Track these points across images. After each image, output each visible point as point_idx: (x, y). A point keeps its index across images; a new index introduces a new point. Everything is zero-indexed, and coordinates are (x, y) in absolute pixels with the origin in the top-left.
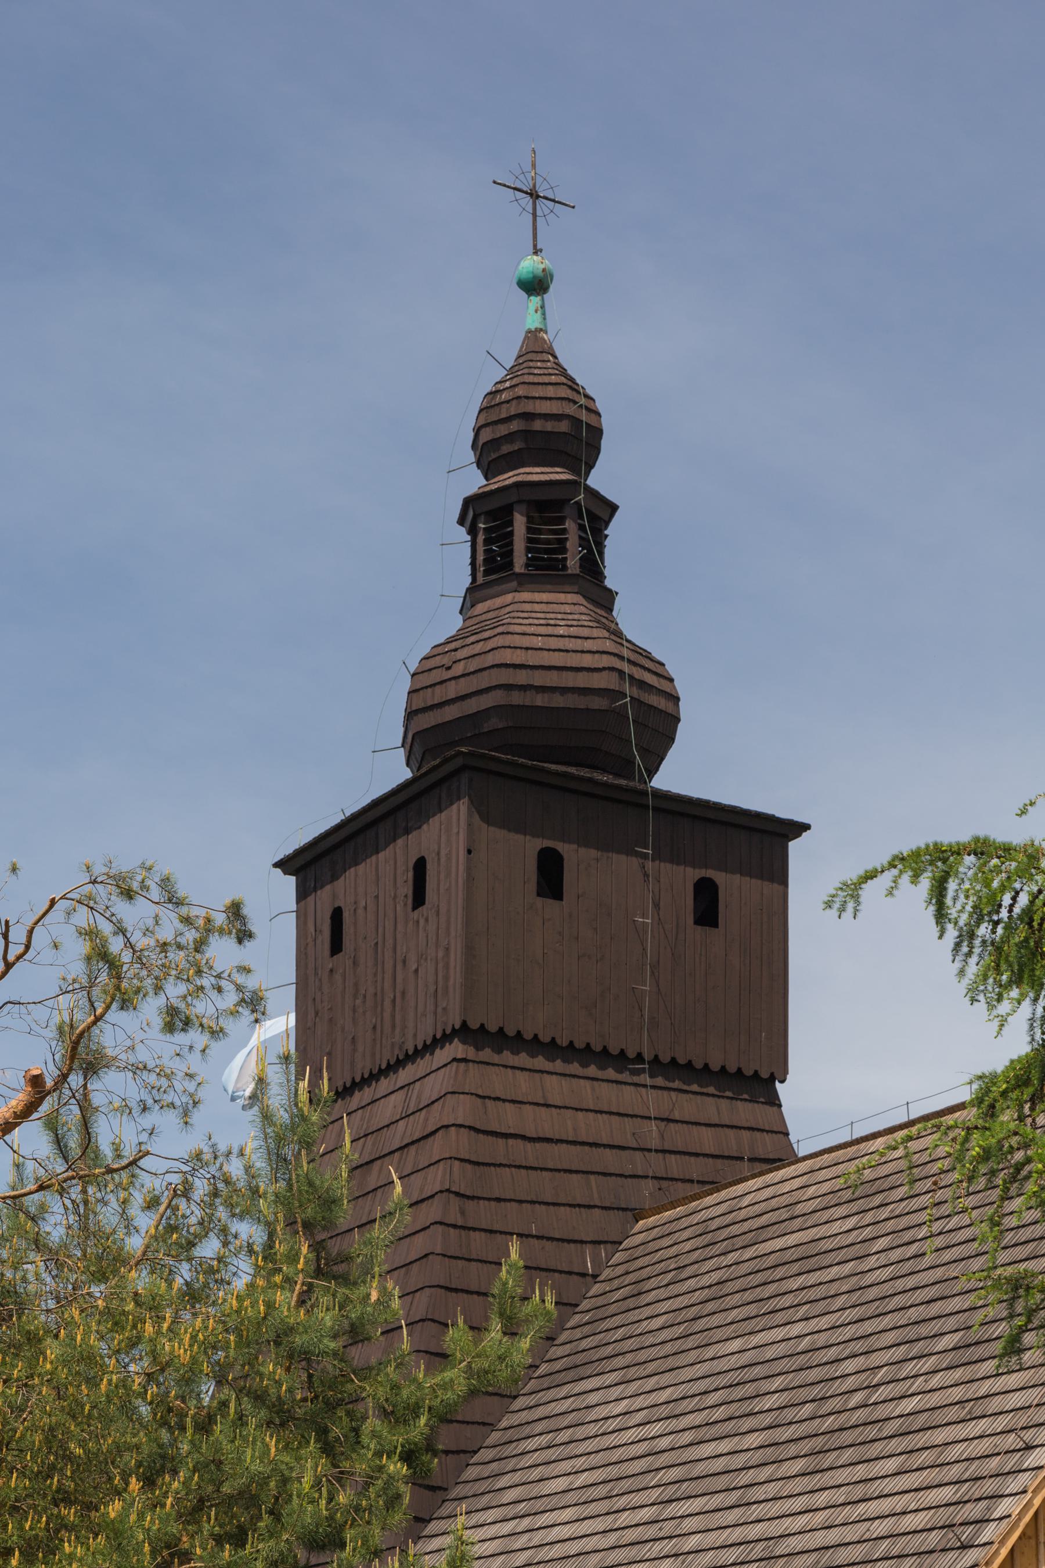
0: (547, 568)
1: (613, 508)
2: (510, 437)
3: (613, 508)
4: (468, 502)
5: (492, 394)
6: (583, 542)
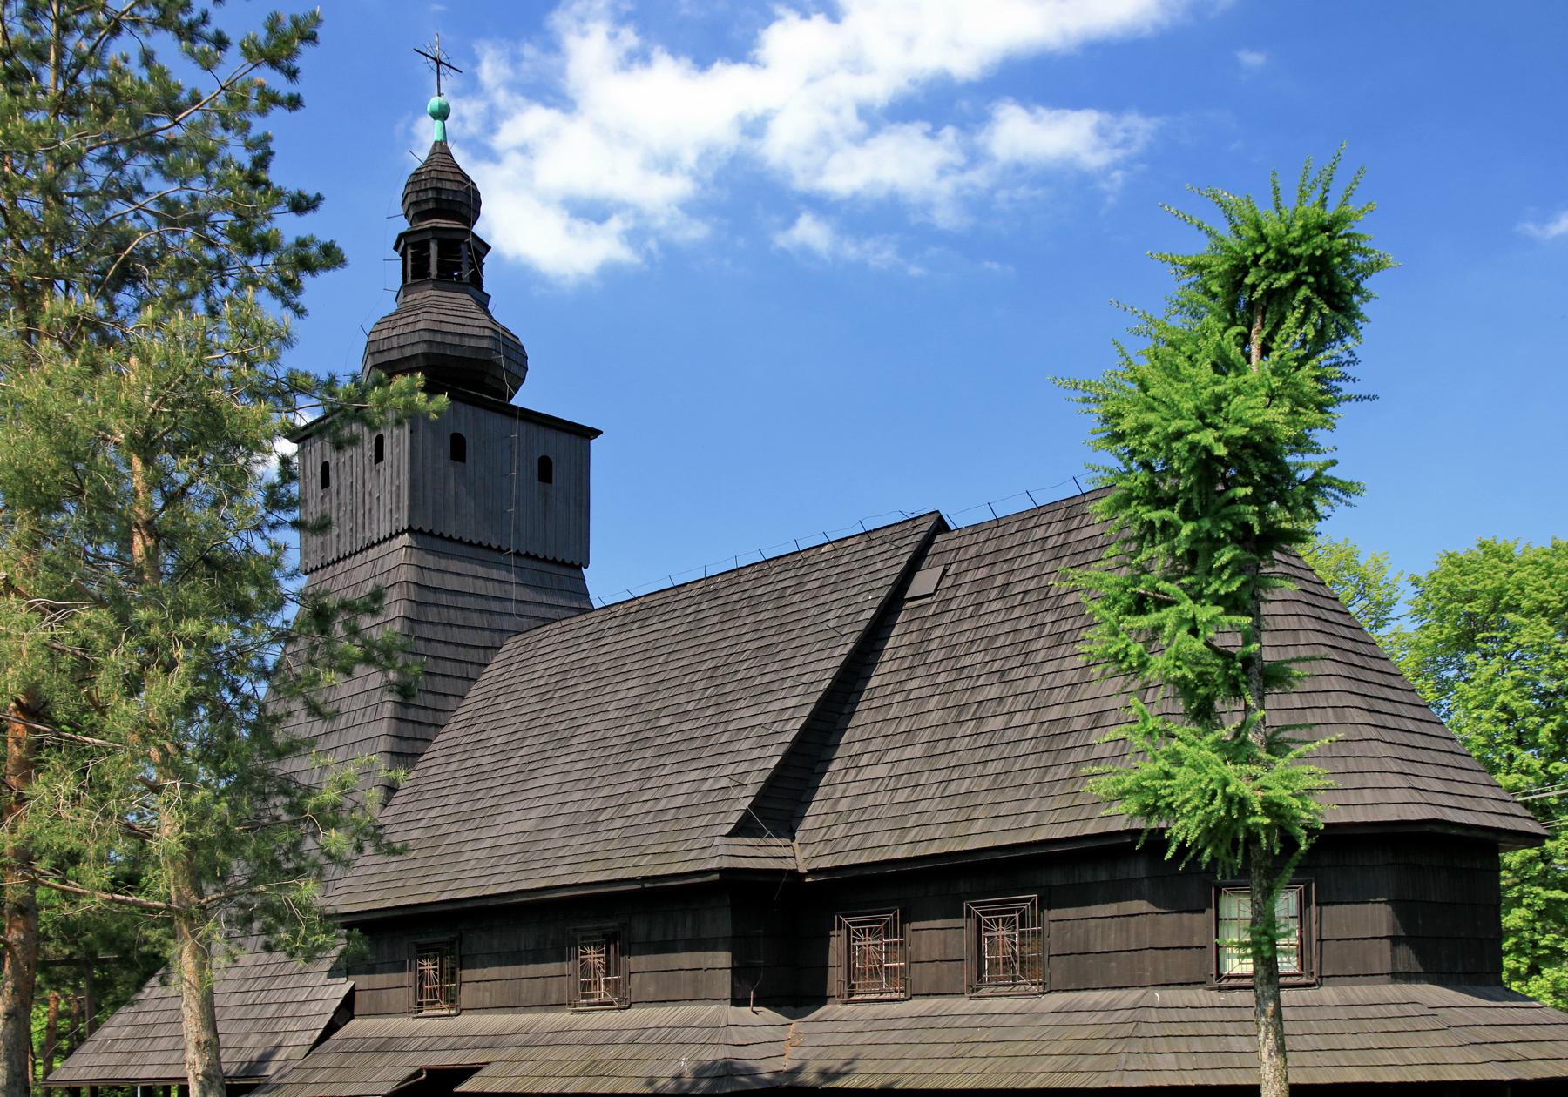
0: (447, 278)
2: (427, 200)
3: (488, 248)
4: (401, 236)
5: (415, 174)
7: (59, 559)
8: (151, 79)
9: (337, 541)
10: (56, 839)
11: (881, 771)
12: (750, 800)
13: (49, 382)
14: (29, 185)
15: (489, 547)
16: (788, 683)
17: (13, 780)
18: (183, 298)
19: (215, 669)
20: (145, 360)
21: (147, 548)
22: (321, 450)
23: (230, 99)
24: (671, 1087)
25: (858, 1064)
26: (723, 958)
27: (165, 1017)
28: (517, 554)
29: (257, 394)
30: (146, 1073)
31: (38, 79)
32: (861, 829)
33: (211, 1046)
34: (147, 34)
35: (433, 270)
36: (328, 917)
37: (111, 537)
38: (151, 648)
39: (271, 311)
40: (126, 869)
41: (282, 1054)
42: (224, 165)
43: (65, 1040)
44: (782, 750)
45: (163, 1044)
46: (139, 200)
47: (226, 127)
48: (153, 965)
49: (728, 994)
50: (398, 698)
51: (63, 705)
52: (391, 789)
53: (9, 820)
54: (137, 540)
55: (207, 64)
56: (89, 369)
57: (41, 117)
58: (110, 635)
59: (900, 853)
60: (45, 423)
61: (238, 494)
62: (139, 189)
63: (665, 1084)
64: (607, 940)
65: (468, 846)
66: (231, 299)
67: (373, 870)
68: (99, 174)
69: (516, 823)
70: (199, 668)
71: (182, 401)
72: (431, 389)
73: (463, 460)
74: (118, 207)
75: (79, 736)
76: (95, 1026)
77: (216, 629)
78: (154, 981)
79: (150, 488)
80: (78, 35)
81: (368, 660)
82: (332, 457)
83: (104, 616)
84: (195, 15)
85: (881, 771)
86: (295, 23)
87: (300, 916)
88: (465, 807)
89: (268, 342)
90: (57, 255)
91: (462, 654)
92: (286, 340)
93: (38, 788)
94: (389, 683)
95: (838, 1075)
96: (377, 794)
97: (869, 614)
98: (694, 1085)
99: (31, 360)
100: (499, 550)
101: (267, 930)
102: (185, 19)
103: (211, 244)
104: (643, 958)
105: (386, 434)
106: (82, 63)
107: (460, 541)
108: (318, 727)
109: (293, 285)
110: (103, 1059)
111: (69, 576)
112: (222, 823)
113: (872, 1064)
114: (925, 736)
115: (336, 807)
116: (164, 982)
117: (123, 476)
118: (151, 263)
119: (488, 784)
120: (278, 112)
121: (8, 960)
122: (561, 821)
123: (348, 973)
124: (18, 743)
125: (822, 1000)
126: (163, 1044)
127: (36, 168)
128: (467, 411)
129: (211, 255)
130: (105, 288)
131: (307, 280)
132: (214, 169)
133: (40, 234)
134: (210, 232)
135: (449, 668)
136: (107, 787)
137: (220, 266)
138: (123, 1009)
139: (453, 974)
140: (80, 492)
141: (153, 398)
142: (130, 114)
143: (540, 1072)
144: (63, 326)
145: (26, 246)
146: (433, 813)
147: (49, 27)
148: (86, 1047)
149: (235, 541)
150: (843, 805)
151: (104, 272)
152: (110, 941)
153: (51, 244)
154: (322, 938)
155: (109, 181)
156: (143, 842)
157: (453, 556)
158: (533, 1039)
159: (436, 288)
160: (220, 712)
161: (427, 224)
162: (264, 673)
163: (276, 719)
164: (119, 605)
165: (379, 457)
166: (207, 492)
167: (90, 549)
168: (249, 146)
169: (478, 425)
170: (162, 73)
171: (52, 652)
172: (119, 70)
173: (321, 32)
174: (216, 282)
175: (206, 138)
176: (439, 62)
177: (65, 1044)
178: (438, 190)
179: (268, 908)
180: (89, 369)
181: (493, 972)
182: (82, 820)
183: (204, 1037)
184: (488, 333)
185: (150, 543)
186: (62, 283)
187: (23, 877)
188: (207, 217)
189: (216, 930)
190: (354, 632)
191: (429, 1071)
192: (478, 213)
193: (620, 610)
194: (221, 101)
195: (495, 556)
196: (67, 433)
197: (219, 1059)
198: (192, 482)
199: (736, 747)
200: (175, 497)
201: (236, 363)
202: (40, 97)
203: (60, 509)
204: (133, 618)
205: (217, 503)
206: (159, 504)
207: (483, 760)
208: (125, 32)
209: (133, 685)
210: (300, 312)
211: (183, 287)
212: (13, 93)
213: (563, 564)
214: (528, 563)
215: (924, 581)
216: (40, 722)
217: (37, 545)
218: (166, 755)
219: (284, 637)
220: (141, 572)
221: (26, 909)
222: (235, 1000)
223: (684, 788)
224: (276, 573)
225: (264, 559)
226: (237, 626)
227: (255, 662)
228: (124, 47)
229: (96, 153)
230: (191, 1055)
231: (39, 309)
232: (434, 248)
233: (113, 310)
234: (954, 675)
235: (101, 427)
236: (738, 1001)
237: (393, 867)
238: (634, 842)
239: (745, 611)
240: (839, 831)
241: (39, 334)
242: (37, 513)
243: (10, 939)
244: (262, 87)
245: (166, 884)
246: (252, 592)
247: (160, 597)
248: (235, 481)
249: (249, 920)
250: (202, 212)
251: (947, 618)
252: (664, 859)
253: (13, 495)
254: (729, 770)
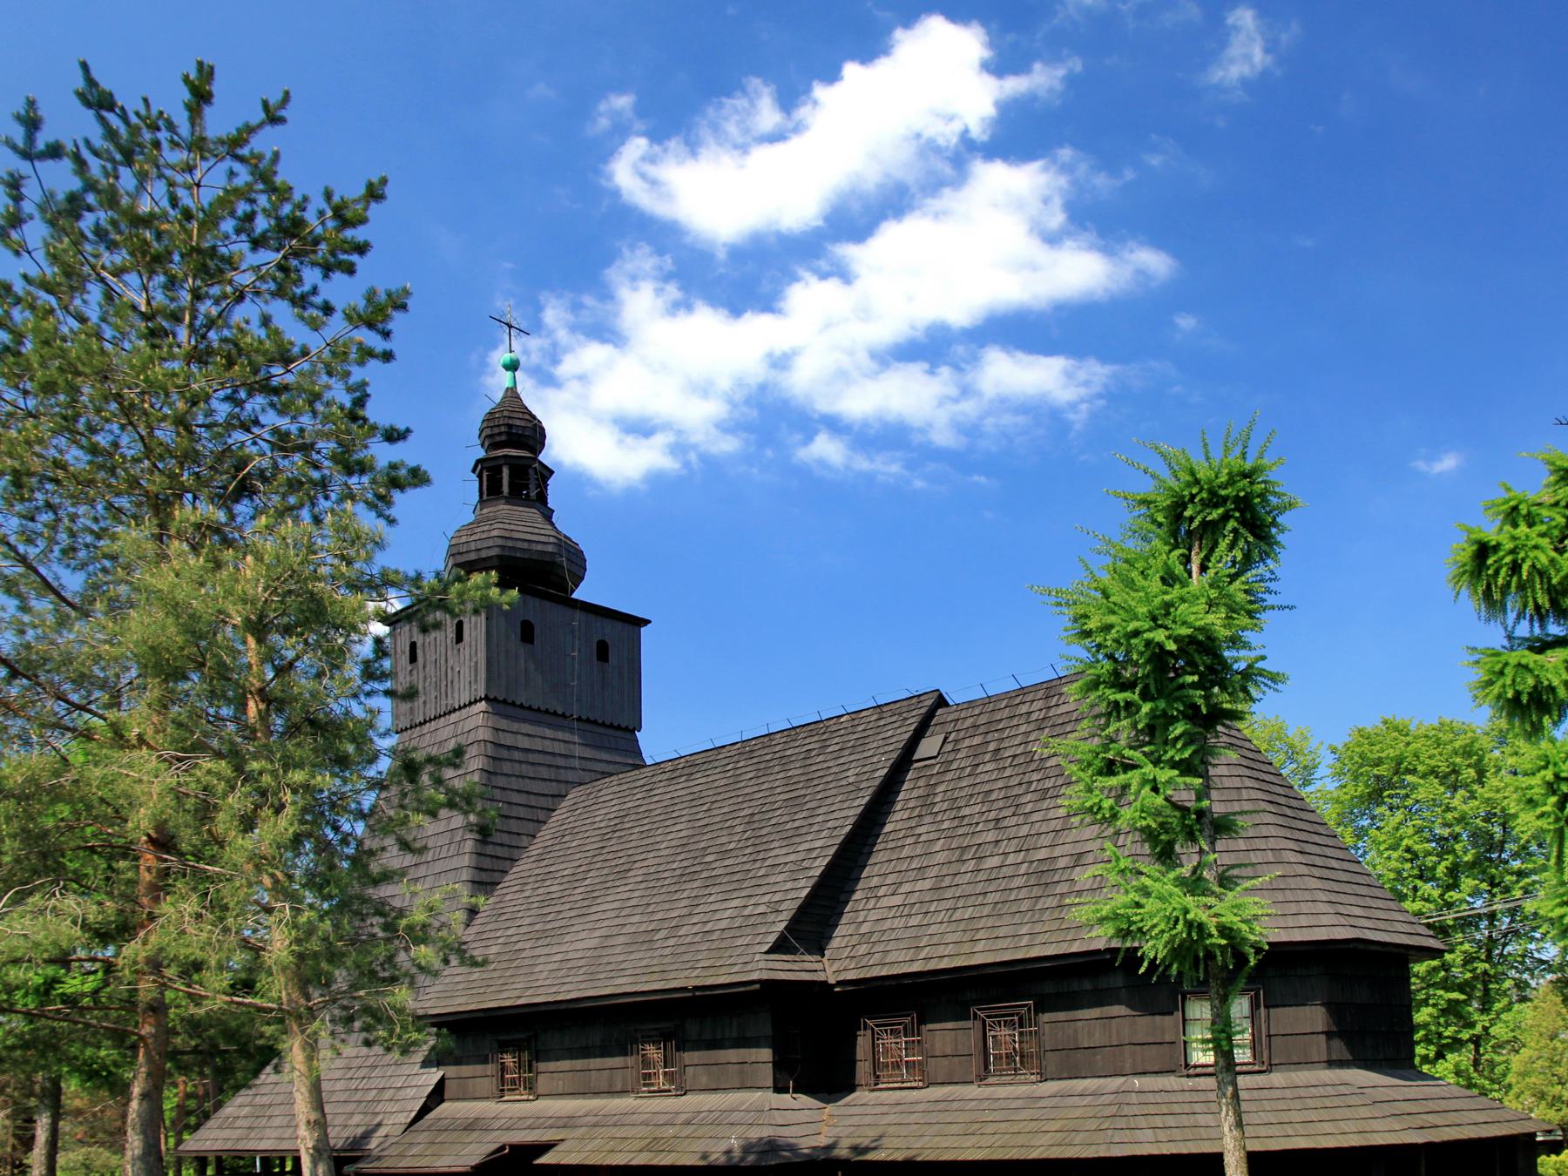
0: (517, 495)
1: (552, 472)
2: (500, 434)
3: (552, 472)
4: (478, 462)
6: (539, 486)
7: (184, 718)
8: (268, 336)
9: (421, 708)
10: (183, 951)
11: (897, 900)
12: (784, 924)
13: (177, 575)
14: (164, 418)
15: (555, 714)
16: (816, 828)
17: (145, 901)
18: (291, 508)
19: (319, 811)
20: (259, 558)
21: (259, 711)
22: (408, 632)
23: (333, 353)
24: (722, 1160)
25: (885, 1141)
26: (766, 1054)
27: (279, 1099)
28: (579, 719)
29: (355, 586)
30: (263, 1145)
31: (175, 336)
32: (881, 947)
33: (320, 1124)
34: (266, 302)
35: (506, 489)
36: (420, 1018)
37: (229, 701)
38: (263, 793)
39: (367, 521)
40: (243, 975)
41: (382, 1132)
42: (328, 404)
43: (195, 1116)
44: (812, 882)
45: (277, 1121)
46: (256, 430)
47: (330, 374)
48: (268, 1055)
49: (770, 1083)
50: (477, 837)
51: (188, 839)
52: (473, 912)
53: (142, 934)
54: (251, 704)
55: (315, 326)
56: (211, 565)
57: (176, 366)
58: (228, 781)
59: (916, 967)
60: (174, 608)
61: (338, 667)
62: (256, 422)
63: (717, 1158)
64: (663, 1038)
65: (541, 960)
66: (333, 511)
67: (458, 979)
68: (222, 410)
69: (581, 941)
70: (305, 810)
71: (290, 592)
72: (504, 584)
73: (532, 642)
74: (239, 436)
75: (202, 865)
76: (218, 1106)
77: (319, 778)
78: (269, 1069)
79: (263, 662)
80: (209, 303)
81: (451, 805)
82: (419, 638)
83: (223, 766)
84: (307, 288)
85: (897, 900)
86: (389, 295)
87: (395, 1017)
88: (537, 927)
89: (364, 545)
90: (186, 474)
91: (533, 801)
92: (379, 544)
93: (166, 908)
94: (470, 824)
95: (867, 1150)
96: (461, 916)
97: (883, 772)
98: (742, 1159)
99: (163, 557)
100: (564, 716)
101: (367, 1028)
102: (298, 291)
103: (316, 467)
104: (696, 1054)
105: (466, 620)
106: (211, 323)
107: (530, 708)
108: (409, 859)
109: (385, 500)
110: (227, 1133)
111: (193, 733)
112: (325, 939)
113: (896, 1140)
114: (934, 872)
115: (424, 926)
116: (277, 1070)
117: (239, 652)
118: (265, 480)
119: (557, 908)
120: (373, 364)
121: (142, 1052)
122: (621, 939)
123: (439, 1064)
124: (149, 869)
125: (851, 1087)
126: (277, 1121)
127: (171, 405)
128: (535, 602)
129: (316, 475)
130: (227, 499)
131: (397, 496)
132: (320, 408)
133: (172, 457)
134: (315, 457)
136: (225, 908)
137: (323, 484)
138: (243, 1092)
139: (530, 1066)
140: (203, 665)
141: (265, 590)
142: (250, 364)
143: (608, 1147)
144: (190, 530)
145: (160, 466)
146: (510, 932)
147: (186, 297)
148: (210, 1123)
149: (335, 706)
150: (864, 928)
151: (225, 488)
152: (230, 1035)
153: (181, 465)
154: (415, 1036)
155: (231, 416)
156: (258, 957)
157: (524, 720)
158: (600, 1122)
159: (508, 503)
160: (323, 847)
161: (500, 453)
162: (361, 815)
163: (371, 853)
164: (236, 757)
165: (459, 638)
166: (312, 666)
167: (211, 711)
168: (349, 390)
169: (544, 614)
170: (277, 332)
171: (179, 796)
172: (241, 330)
173: (410, 302)
174: (320, 496)
175: (314, 383)
176: (510, 327)
177: (192, 1120)
178: (510, 426)
179: (367, 1010)
180: (211, 565)
181: (565, 1064)
182: (204, 935)
183: (313, 1116)
184: (552, 540)
185: (262, 706)
186: (190, 496)
187: (154, 981)
188: (313, 445)
189: (322, 1027)
190: (438, 782)
191: (513, 1147)
192: (543, 445)
193: (669, 767)
194: (326, 355)
196: (192, 617)
197: (326, 1135)
198: (298, 658)
199: (772, 879)
200: (284, 670)
201: (336, 562)
202: (176, 350)
203: (187, 678)
204: (247, 768)
205: (319, 675)
206: (271, 675)
207: (553, 889)
208: (247, 300)
209: (248, 823)
210: (391, 521)
211: (292, 500)
212: (153, 347)
213: (619, 728)
214: (589, 727)
215: (928, 746)
216: (168, 853)
217: (165, 707)
218: (276, 881)
219: (379, 785)
220: (254, 731)
221: (157, 1008)
222: (340, 1085)
223: (728, 913)
224: (371, 733)
225: (359, 721)
226: (337, 775)
227: (353, 806)
228: (246, 312)
229: (222, 394)
230: (303, 1131)
231: (170, 516)
232: (506, 472)
233: (232, 517)
234: (956, 823)
235: (220, 612)
236: (779, 1089)
237: (475, 976)
238: (685, 957)
239: (777, 769)
240: (863, 949)
241: (169, 537)
242: (166, 681)
243: (143, 1032)
244: (360, 344)
245: (277, 989)
246: (351, 748)
247: (271, 752)
248: (335, 658)
249: (350, 1020)
250: (308, 441)
251: (949, 776)
252: (711, 971)
253: (146, 666)
254: (766, 899)
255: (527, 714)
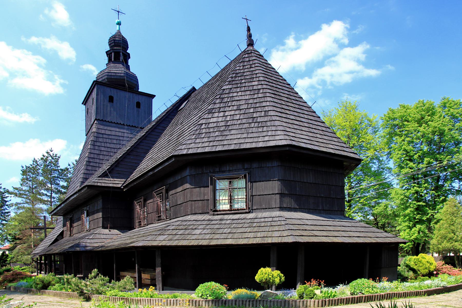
2: (112, 43)
35: (113, 60)
73: (113, 102)
100: (123, 124)
107: (111, 122)
135: (105, 153)
157: (109, 126)
176: (119, 12)
195: (122, 126)
232: (113, 54)
255: (111, 124)
